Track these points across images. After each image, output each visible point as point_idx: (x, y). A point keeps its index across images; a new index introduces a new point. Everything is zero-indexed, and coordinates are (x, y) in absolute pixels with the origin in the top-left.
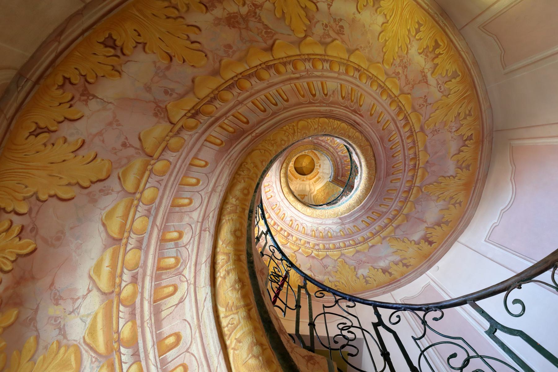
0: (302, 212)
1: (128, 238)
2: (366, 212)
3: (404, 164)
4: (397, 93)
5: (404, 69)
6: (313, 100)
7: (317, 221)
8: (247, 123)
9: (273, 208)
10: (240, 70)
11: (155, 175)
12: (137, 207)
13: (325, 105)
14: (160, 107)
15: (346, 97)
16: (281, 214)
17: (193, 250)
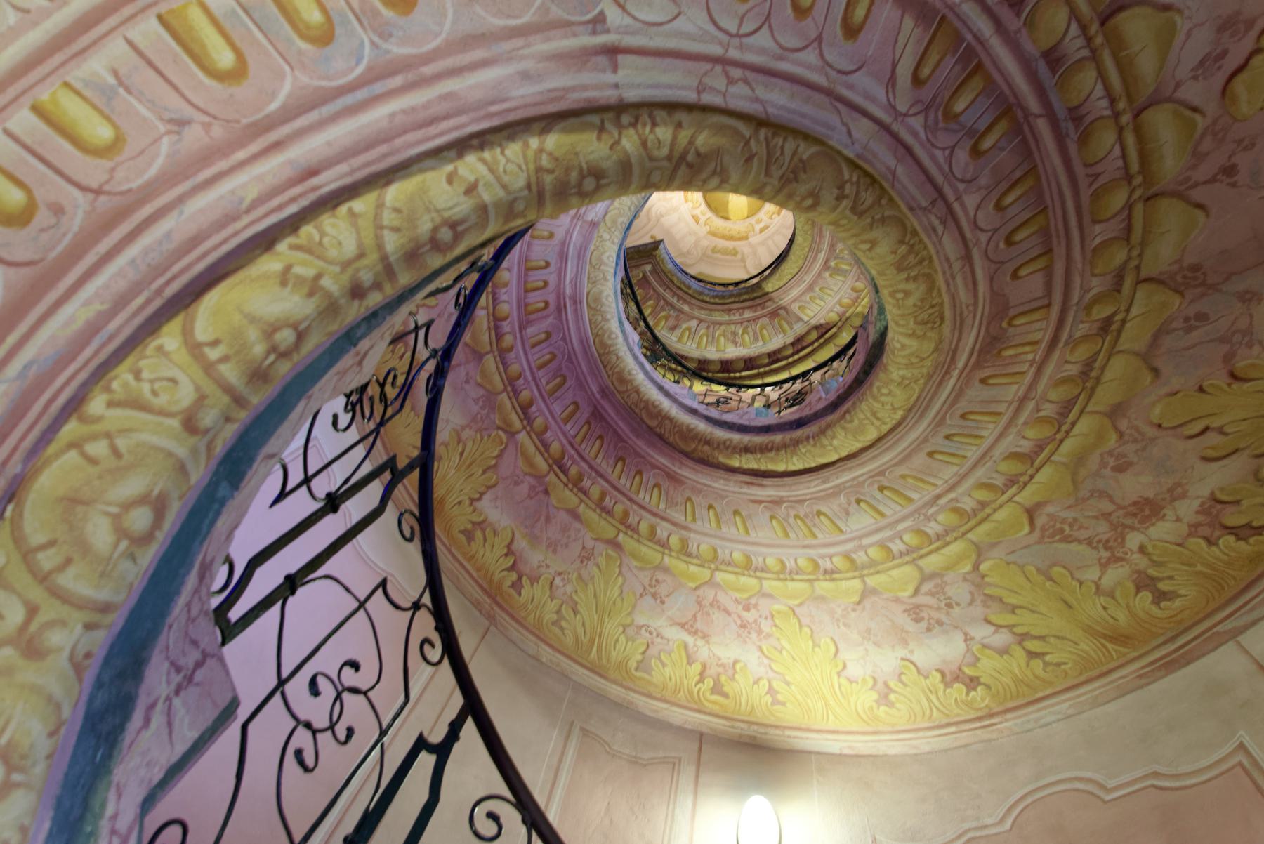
1: (1089, 40)
2: (560, 296)
3: (587, 457)
4: (720, 576)
5: (742, 621)
6: (879, 481)
12: (1113, 101)
13: (848, 485)
15: (813, 516)
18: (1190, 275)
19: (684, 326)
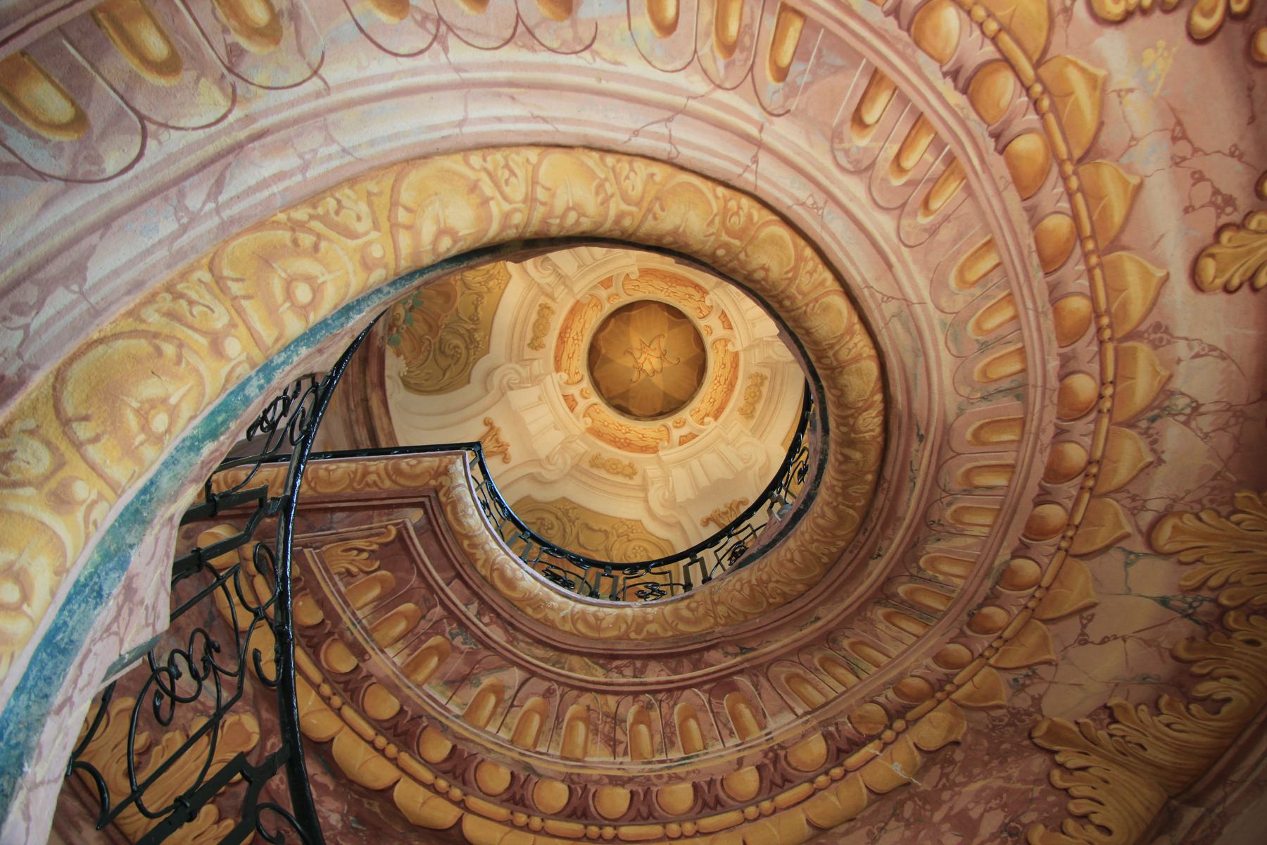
0: (518, 159)
7: (287, 162)
19: (487, 681)
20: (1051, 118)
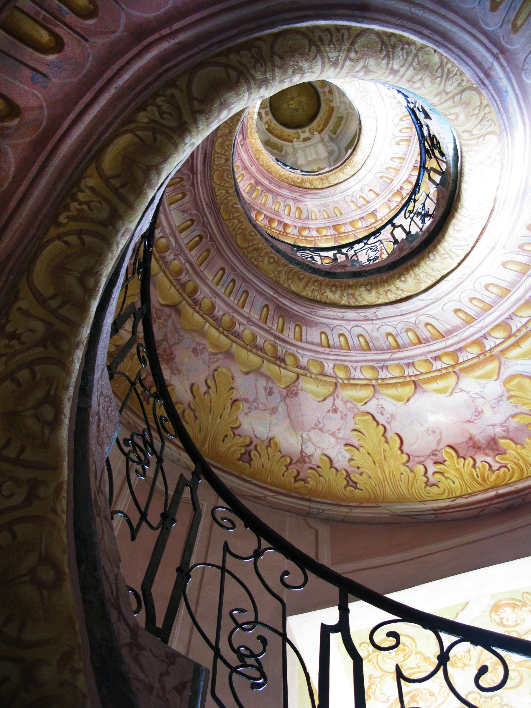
1: (410, 376)
6: (207, 237)
8: (266, 306)
9: (390, 182)
10: (214, 332)
11: (350, 374)
12: (383, 379)
13: (205, 218)
14: (287, 394)
15: (181, 190)
16: (395, 164)
17: (395, 321)
18: (294, 392)
20: (364, 229)
